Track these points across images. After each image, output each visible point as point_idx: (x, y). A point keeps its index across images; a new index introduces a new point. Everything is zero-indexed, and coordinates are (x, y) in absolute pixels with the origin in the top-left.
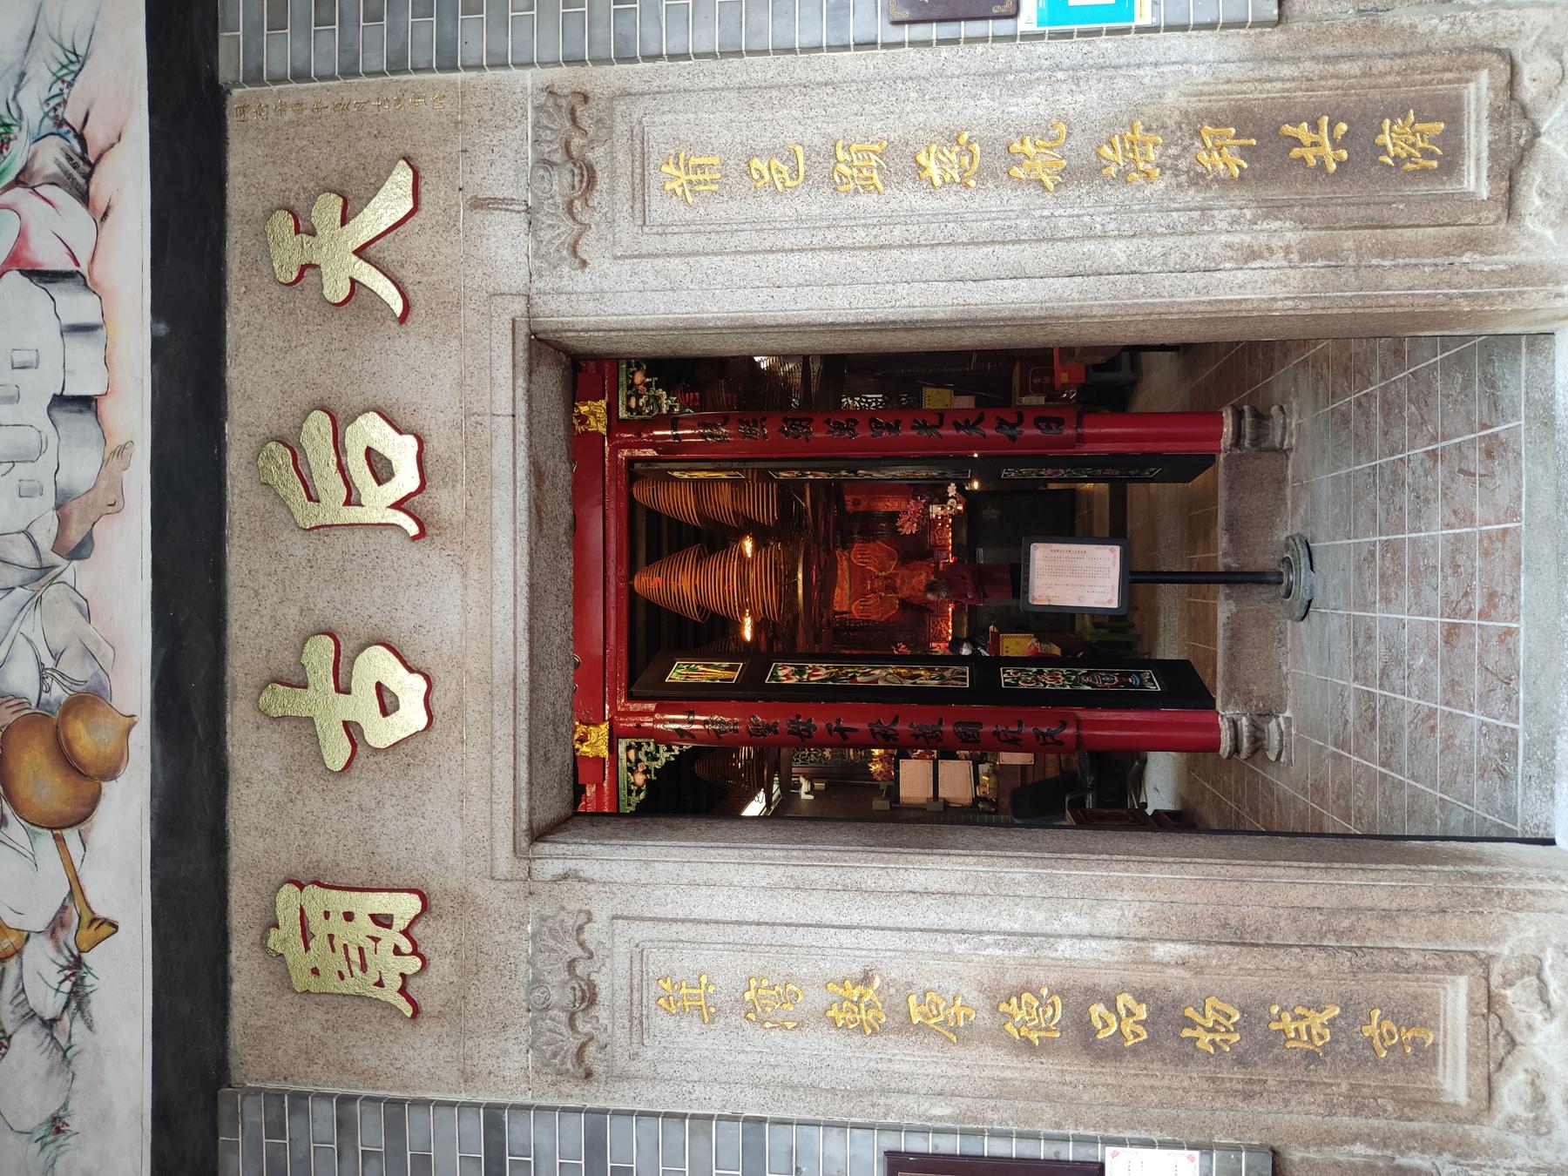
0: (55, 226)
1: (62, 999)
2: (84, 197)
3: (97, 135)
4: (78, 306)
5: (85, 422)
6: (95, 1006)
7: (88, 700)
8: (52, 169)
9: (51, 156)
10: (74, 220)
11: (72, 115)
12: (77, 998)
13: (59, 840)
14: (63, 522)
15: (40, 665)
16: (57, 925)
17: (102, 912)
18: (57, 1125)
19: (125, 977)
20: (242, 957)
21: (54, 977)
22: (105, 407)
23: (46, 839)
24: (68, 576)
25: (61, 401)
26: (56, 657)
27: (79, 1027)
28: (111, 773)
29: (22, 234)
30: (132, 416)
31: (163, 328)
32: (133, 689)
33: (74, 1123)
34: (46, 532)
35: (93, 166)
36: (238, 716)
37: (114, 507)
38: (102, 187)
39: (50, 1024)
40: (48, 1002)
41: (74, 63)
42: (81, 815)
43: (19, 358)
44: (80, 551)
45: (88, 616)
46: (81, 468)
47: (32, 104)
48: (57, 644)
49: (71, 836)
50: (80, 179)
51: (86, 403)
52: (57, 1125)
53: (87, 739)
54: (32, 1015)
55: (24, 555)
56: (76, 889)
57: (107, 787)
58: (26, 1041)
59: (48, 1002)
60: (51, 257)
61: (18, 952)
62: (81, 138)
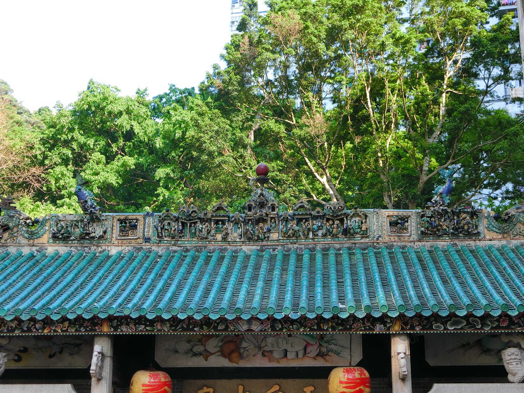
0: (313, 350)
1: (195, 352)
2: (317, 355)
3: (327, 358)
4: (301, 355)
5: (282, 356)
6: (194, 357)
7: (241, 357)
8: (322, 350)
9: (324, 350)
10: (314, 354)
11: (330, 353)
12: (195, 355)
13: (219, 351)
14: (268, 352)
15: (245, 348)
16: (206, 351)
17: (209, 358)
18: (176, 352)
19: (198, 362)
20: (203, 382)
21: (199, 350)
22: (285, 359)
23: (218, 349)
24: (260, 352)
25: (286, 351)
26: (247, 350)
27: (190, 355)
28: (230, 360)
29: (312, 345)
30: (283, 364)
31: (297, 369)
32: (243, 364)
33: (177, 355)
34: (266, 348)
35: (322, 357)
36: (239, 381)
37: (270, 361)
38: (319, 358)
39: (191, 350)
40: (195, 350)
41: (338, 354)
42: (224, 355)
43: (293, 344)
44: (263, 355)
45: (253, 356)
46: (276, 355)
47: (332, 347)
48: (249, 351)
49: (220, 353)
50: (321, 355)
51: (286, 356)
52: (176, 352)
53: (235, 355)
54: (193, 347)
55: (263, 345)
56: (212, 354)
57: (227, 360)
58: (188, 346)
59: (195, 350)
60: (308, 350)
61: (202, 345)
62: (326, 355)
